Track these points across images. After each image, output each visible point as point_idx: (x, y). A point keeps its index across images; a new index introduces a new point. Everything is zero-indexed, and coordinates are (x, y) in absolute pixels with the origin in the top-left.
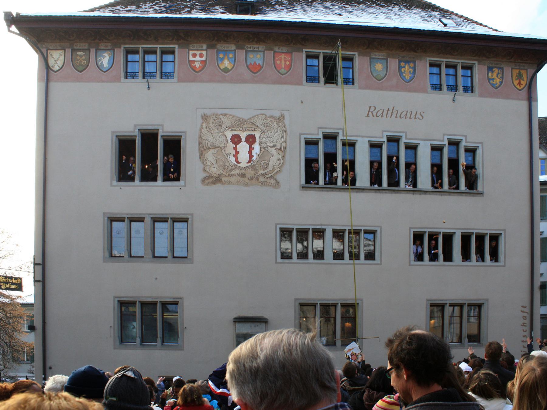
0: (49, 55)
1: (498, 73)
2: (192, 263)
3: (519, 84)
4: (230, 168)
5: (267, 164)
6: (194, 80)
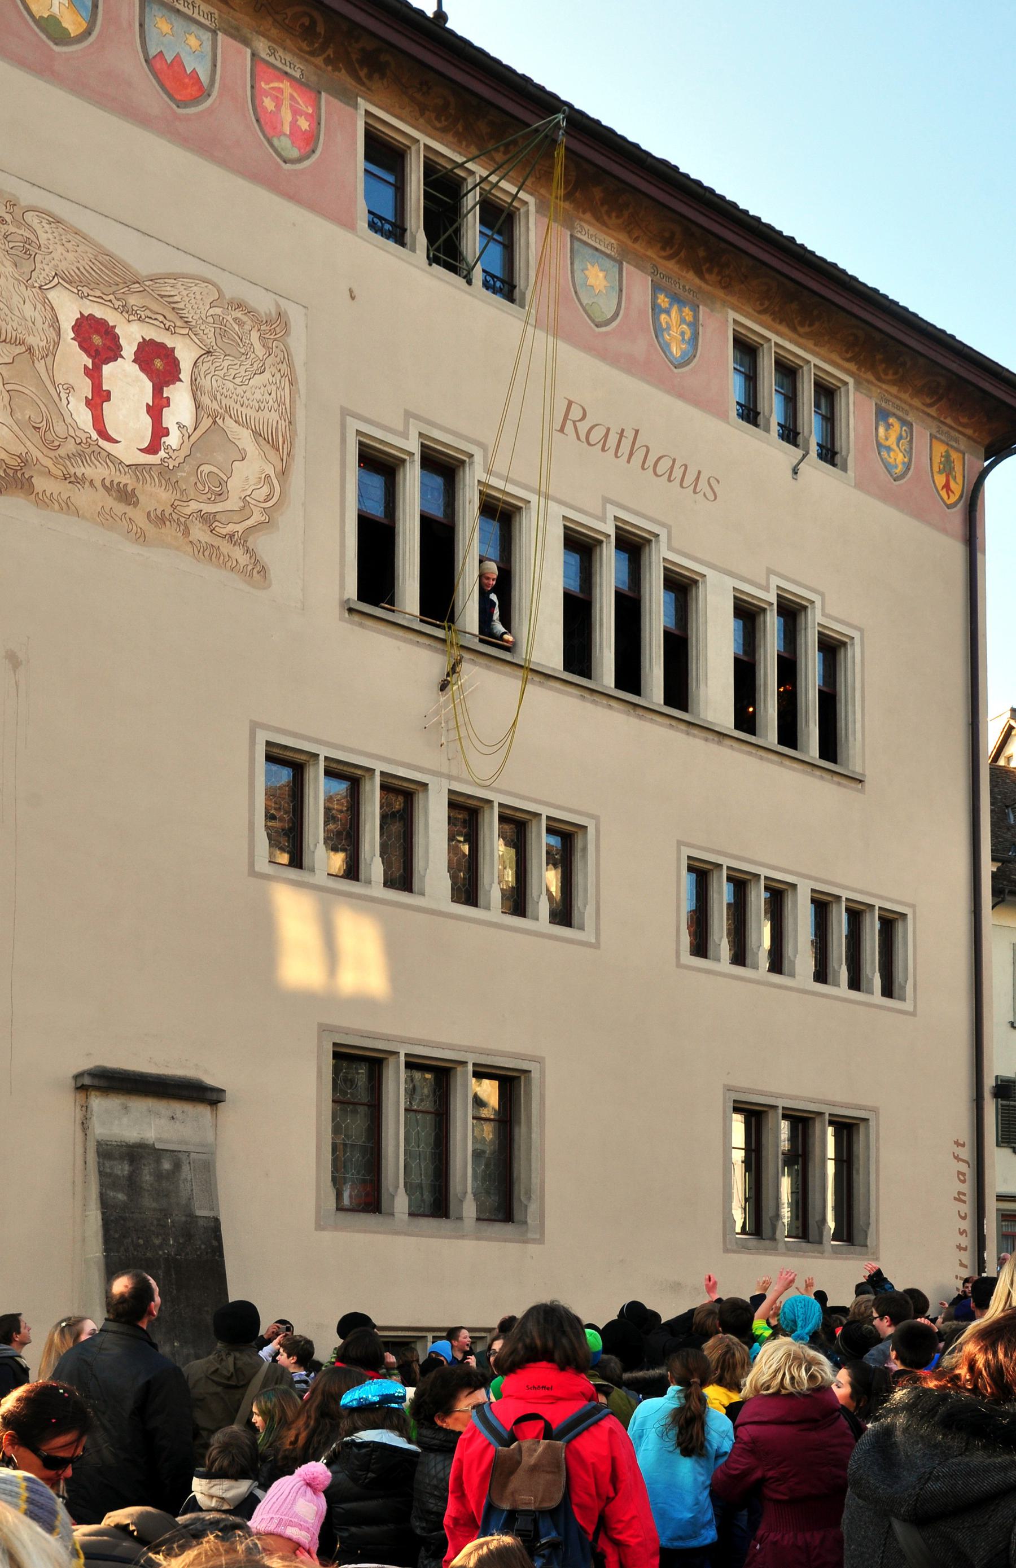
4: (70, 447)
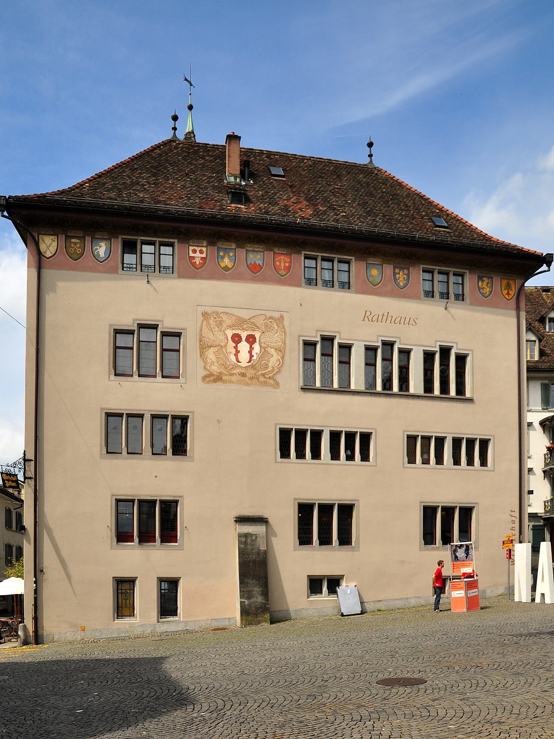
0: (40, 240)
1: (488, 283)
2: (193, 461)
3: (508, 294)
4: (231, 367)
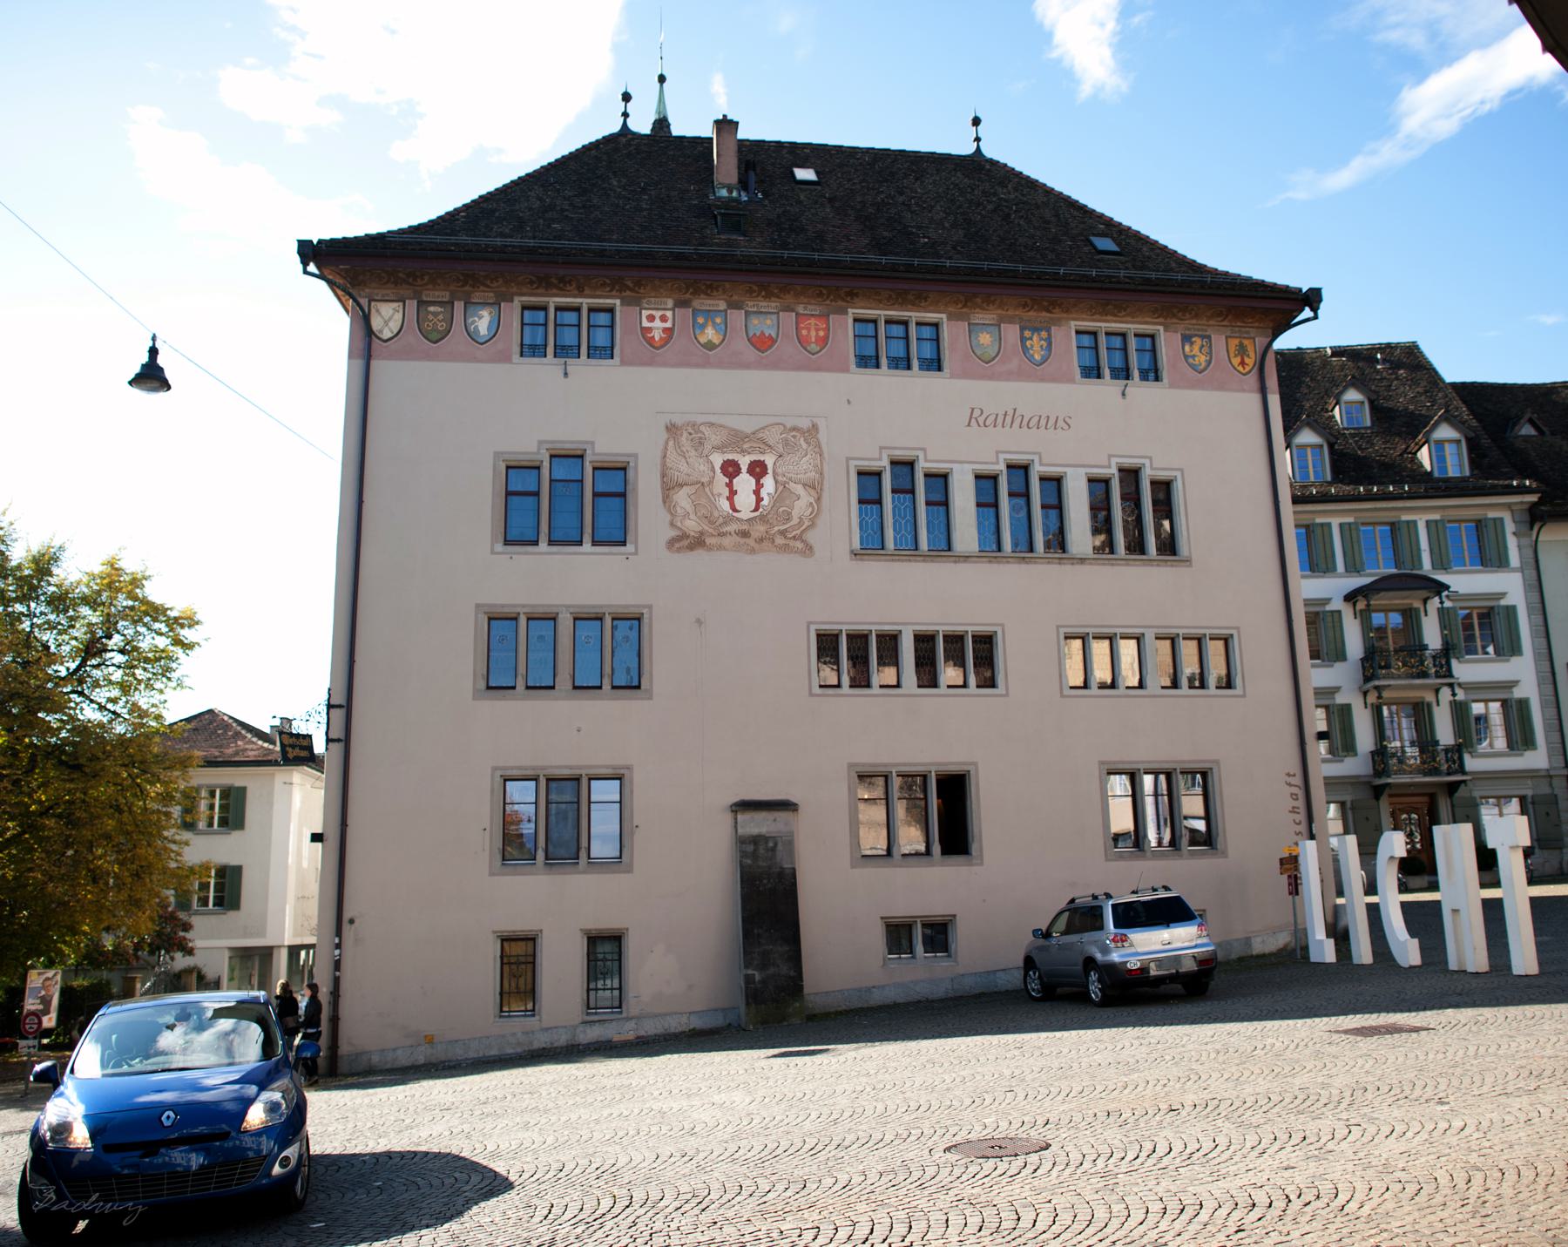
2: (651, 698)
3: (1243, 363)
5: (789, 514)
6: (650, 362)
